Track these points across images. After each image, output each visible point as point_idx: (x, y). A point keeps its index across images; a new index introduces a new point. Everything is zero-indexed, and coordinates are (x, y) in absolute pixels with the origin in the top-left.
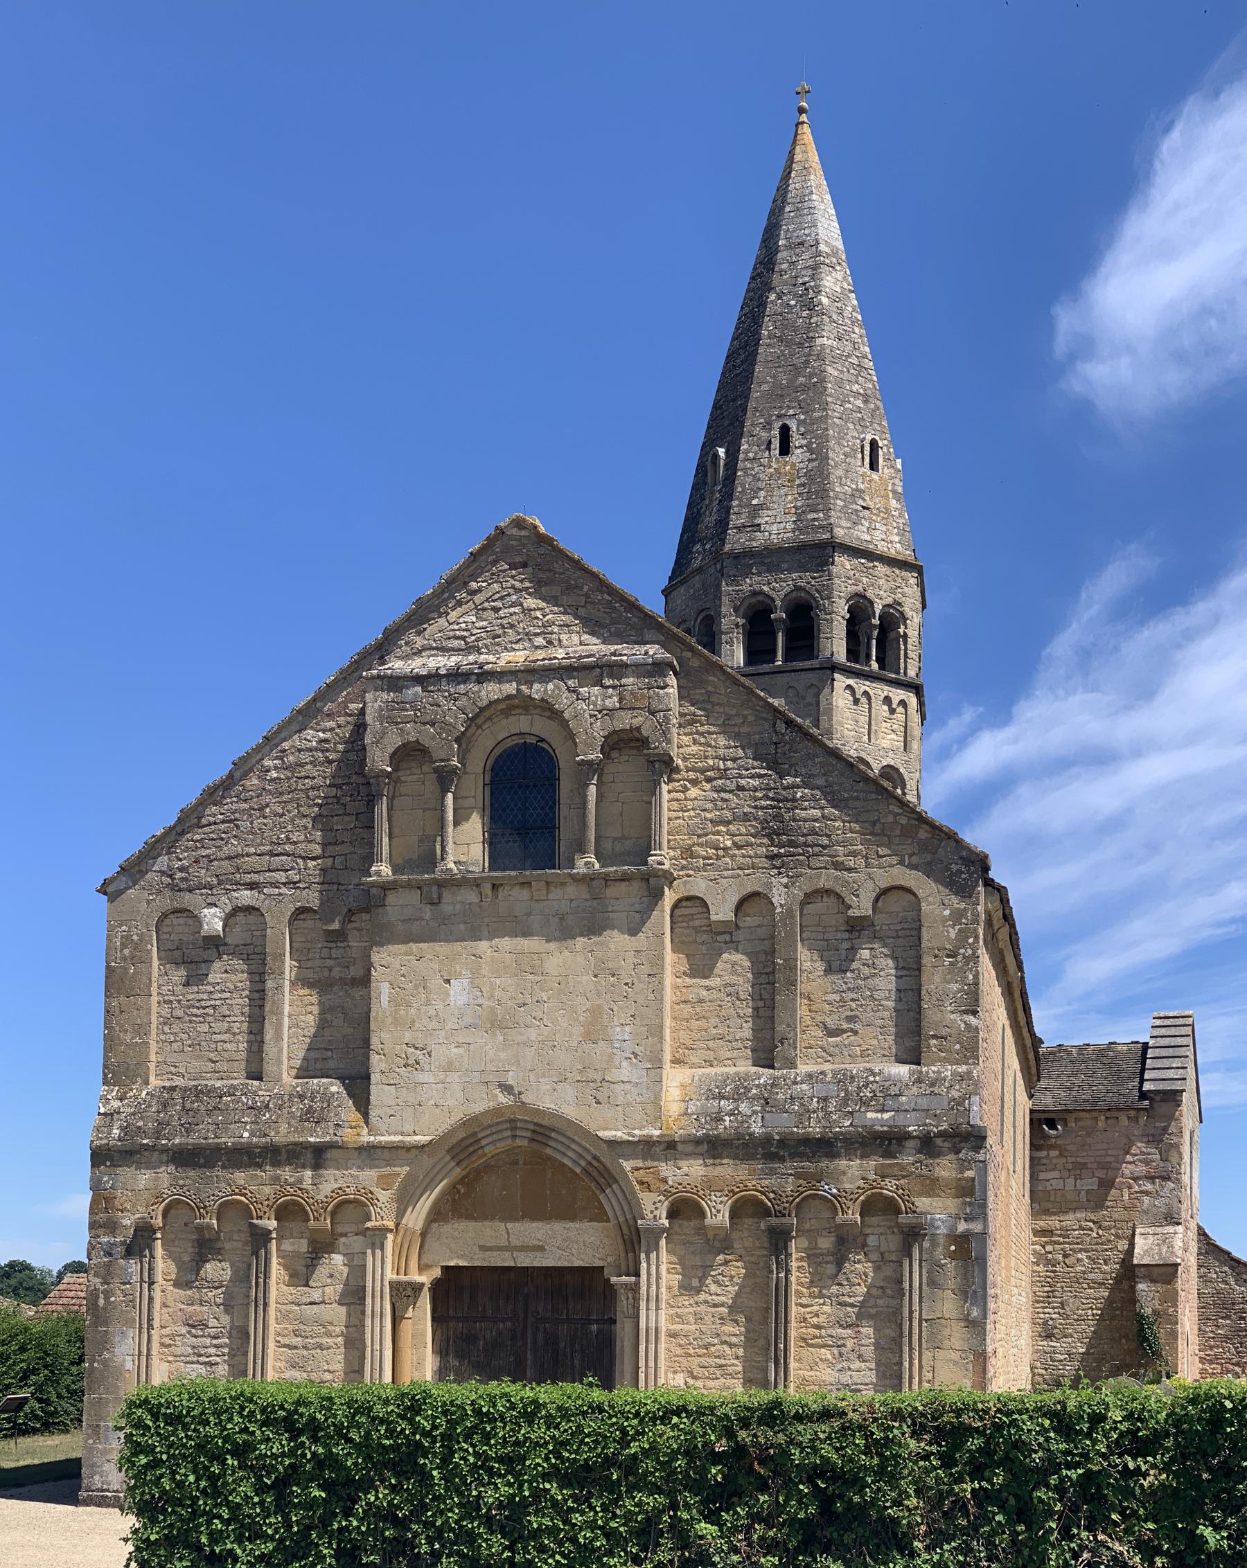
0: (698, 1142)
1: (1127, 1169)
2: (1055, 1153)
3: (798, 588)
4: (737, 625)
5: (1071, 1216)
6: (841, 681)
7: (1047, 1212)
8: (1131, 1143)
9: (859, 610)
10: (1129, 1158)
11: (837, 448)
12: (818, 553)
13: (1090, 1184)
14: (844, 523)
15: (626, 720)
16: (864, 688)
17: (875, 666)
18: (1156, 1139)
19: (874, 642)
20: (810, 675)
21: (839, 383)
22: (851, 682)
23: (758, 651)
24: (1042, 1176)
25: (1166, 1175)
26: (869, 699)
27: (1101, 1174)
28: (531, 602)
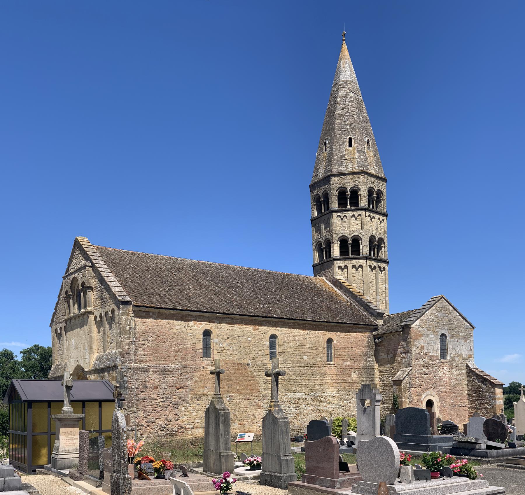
0: (93, 370)
1: (399, 350)
2: (383, 347)
3: (325, 191)
4: (314, 205)
5: (387, 366)
6: (335, 215)
7: (382, 365)
8: (399, 342)
9: (342, 193)
10: (399, 347)
11: (337, 144)
12: (327, 179)
13: (391, 356)
14: (336, 167)
15: (83, 279)
16: (344, 215)
17: (349, 207)
18: (405, 340)
19: (349, 200)
20: (328, 215)
21: (341, 123)
22: (339, 214)
23: (319, 211)
24: (380, 354)
25: (408, 352)
26: (347, 217)
27: (393, 352)
28: (80, 255)
